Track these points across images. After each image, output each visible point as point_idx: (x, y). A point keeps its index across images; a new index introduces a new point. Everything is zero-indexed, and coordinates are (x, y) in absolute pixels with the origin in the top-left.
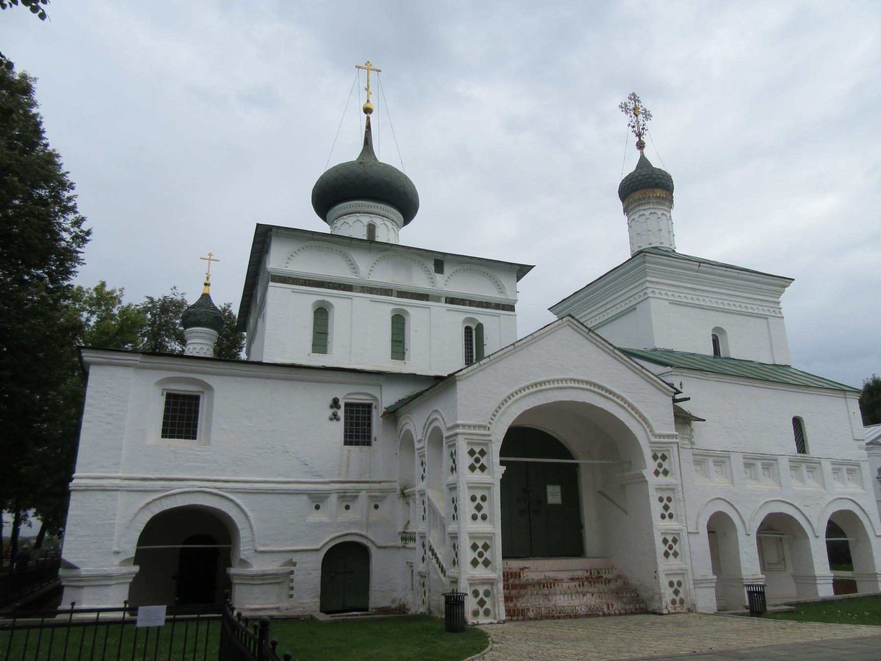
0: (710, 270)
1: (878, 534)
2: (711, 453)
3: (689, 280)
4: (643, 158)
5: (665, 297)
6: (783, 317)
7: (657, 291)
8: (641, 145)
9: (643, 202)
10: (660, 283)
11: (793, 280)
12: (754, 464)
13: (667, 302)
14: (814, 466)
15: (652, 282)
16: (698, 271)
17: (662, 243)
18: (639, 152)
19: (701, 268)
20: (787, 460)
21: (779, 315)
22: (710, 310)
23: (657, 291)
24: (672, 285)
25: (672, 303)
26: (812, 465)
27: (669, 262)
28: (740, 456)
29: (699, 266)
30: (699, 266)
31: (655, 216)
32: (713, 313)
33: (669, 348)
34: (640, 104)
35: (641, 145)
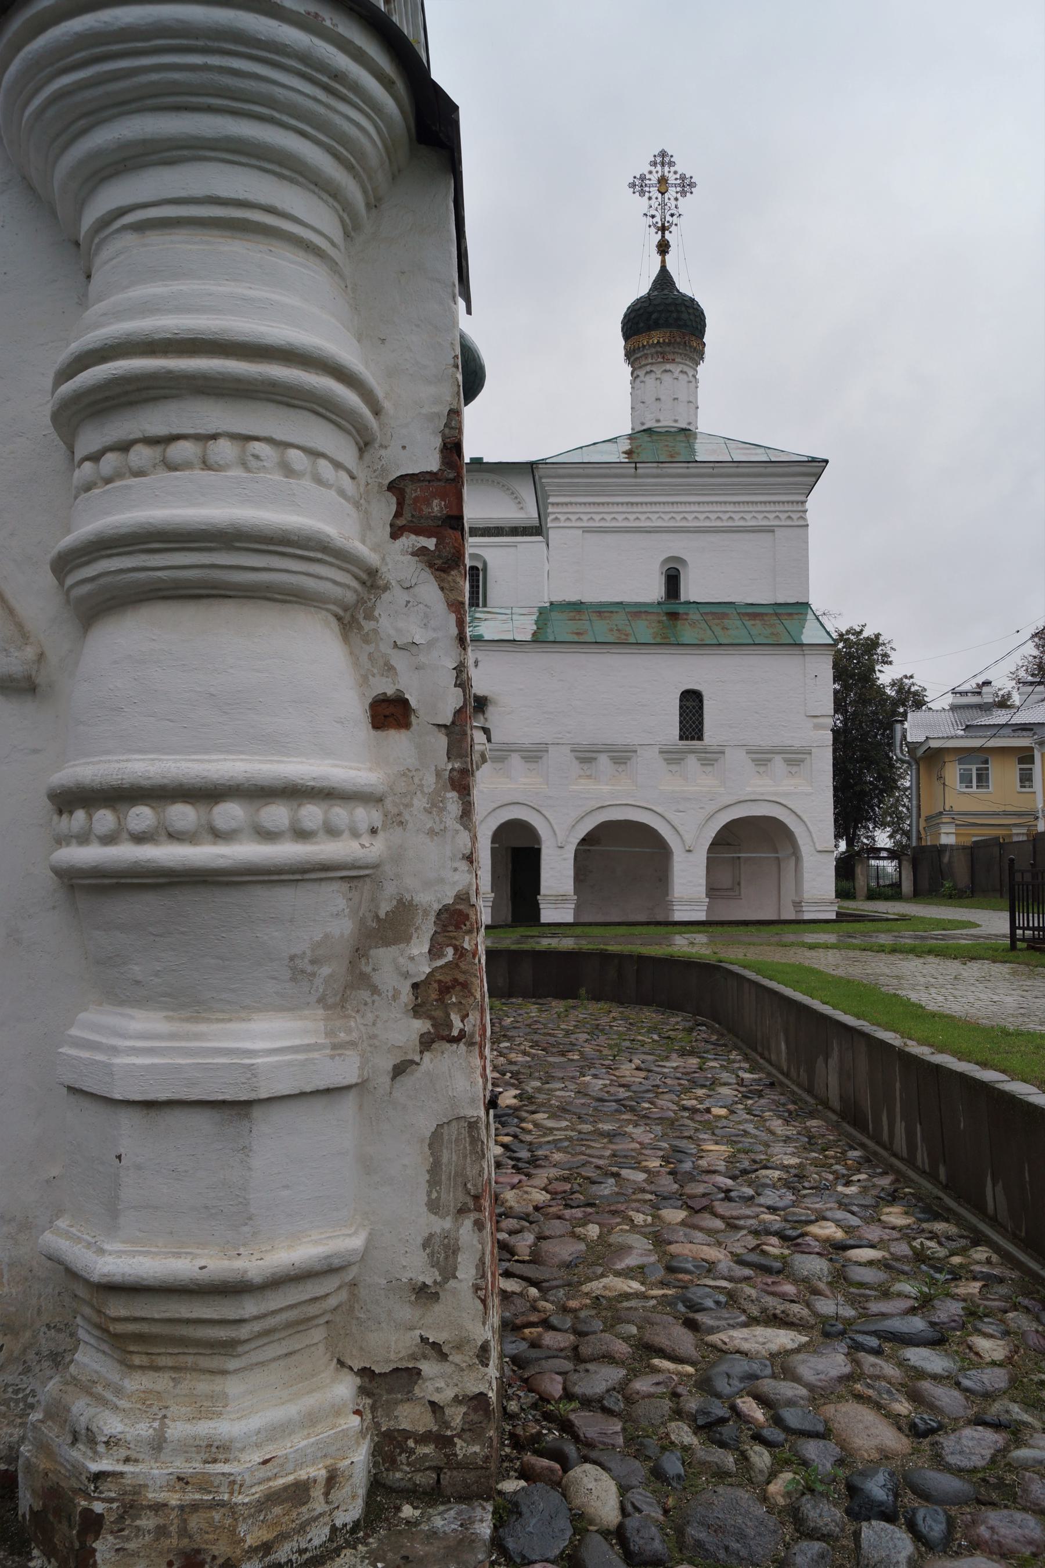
0: (655, 471)
1: (819, 849)
2: (514, 747)
3: (622, 491)
4: (663, 269)
5: (579, 524)
6: (807, 525)
7: (562, 517)
8: (663, 248)
9: (638, 355)
10: (571, 503)
11: (827, 462)
12: (595, 759)
13: (580, 531)
14: (711, 758)
15: (557, 504)
16: (636, 476)
17: (658, 421)
18: (659, 258)
19: (639, 471)
20: (657, 750)
21: (802, 523)
22: (657, 532)
23: (562, 517)
24: (594, 504)
25: (587, 530)
26: (708, 755)
27: (581, 471)
28: (566, 750)
29: (636, 468)
30: (636, 468)
31: (653, 375)
32: (665, 536)
33: (574, 598)
34: (673, 169)
35: (663, 248)
